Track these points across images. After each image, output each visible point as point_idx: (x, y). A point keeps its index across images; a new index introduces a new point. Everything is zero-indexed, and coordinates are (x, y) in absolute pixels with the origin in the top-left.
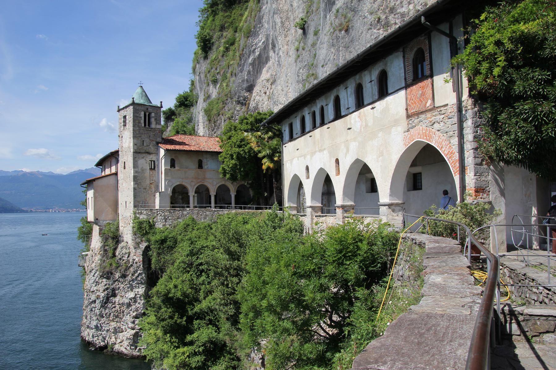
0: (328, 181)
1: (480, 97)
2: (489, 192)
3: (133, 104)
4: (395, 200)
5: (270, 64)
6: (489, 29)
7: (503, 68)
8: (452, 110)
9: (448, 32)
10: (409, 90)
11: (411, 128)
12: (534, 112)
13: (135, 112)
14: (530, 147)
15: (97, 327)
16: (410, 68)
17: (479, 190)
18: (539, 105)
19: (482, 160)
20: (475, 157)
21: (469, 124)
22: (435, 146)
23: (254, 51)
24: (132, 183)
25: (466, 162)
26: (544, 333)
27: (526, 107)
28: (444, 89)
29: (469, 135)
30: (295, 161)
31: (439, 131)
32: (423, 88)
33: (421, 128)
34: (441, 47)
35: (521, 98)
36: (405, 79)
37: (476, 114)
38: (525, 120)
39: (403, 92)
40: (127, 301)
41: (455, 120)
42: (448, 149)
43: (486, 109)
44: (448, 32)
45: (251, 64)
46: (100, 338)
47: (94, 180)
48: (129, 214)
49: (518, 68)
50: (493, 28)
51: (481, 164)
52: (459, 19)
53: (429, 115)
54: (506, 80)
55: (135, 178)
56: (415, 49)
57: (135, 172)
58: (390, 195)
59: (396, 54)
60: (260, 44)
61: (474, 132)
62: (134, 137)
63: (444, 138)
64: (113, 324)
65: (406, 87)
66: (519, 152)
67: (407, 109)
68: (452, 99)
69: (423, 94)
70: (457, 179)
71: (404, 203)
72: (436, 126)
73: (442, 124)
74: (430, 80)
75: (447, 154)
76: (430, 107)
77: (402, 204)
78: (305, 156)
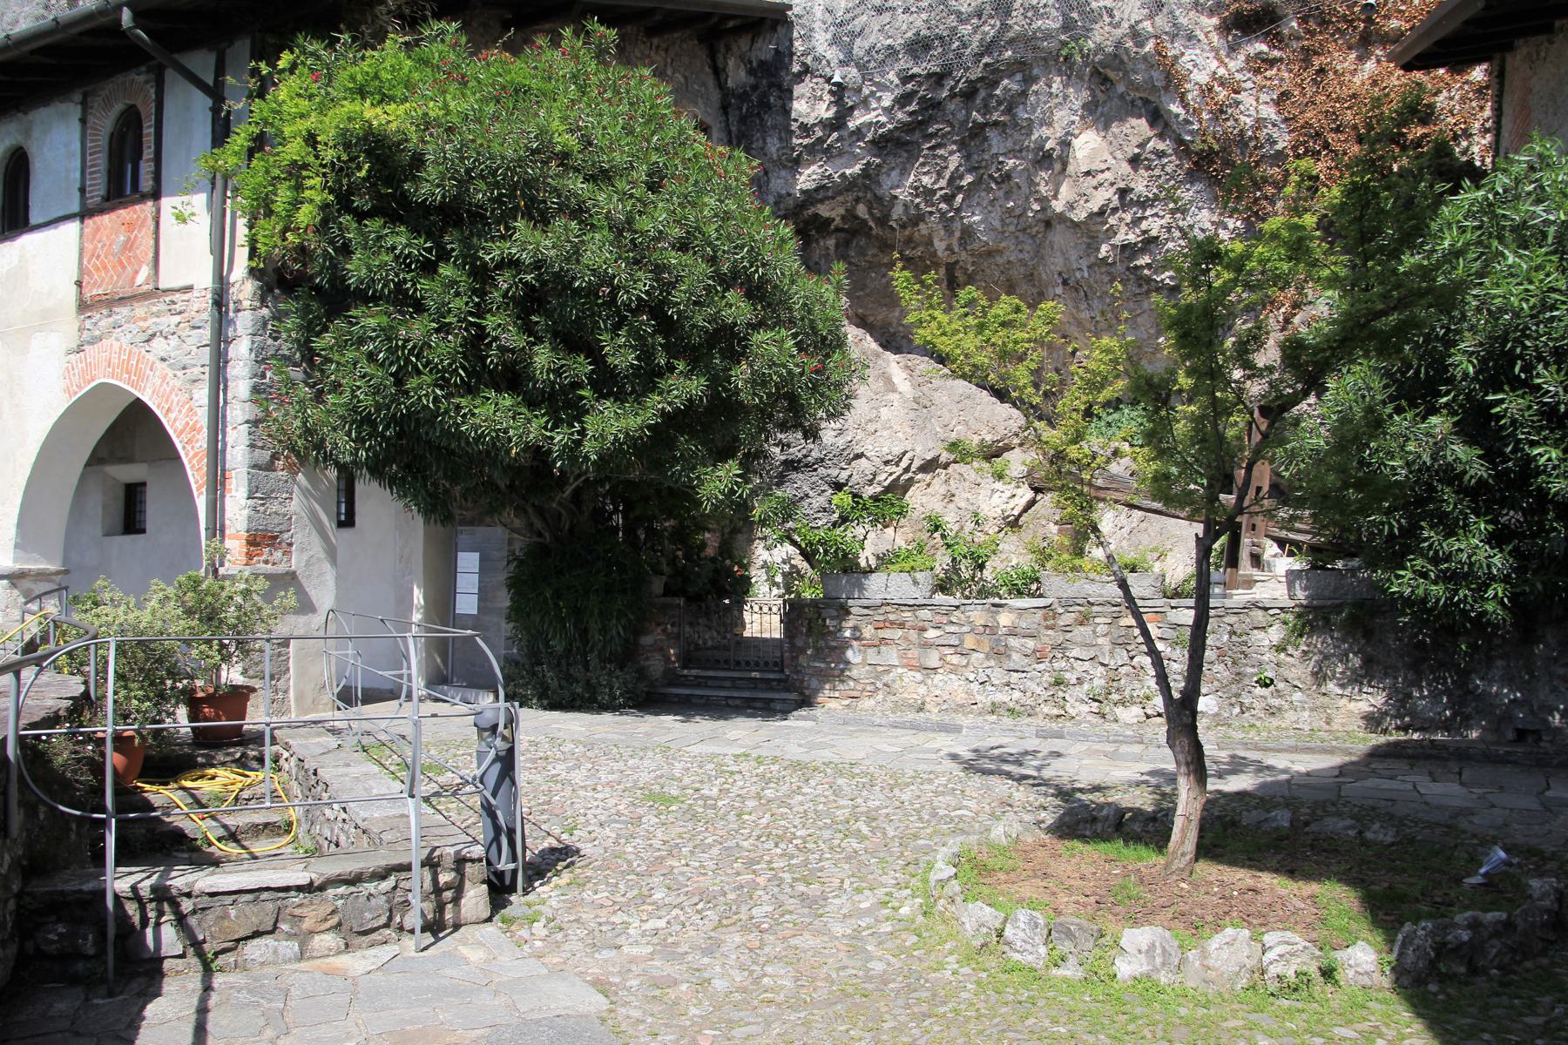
1: (276, 280)
2: (291, 545)
4: (36, 561)
6: (299, 95)
7: (325, 207)
8: (201, 304)
9: (210, 82)
10: (89, 222)
11: (89, 343)
12: (389, 339)
14: (387, 427)
16: (101, 162)
17: (259, 540)
18: (402, 322)
19: (275, 457)
20: (252, 446)
21: (241, 350)
22: (150, 404)
25: (228, 457)
26: (247, 938)
27: (372, 322)
28: (187, 239)
29: (240, 382)
31: (163, 360)
32: (130, 226)
33: (116, 345)
34: (186, 113)
35: (365, 297)
36: (82, 190)
37: (265, 324)
38: (371, 357)
39: (73, 227)
41: (206, 334)
42: (182, 416)
43: (287, 314)
44: (210, 82)
49: (360, 216)
50: (311, 97)
51: (270, 467)
52: (243, 46)
53: (140, 309)
54: (332, 242)
56: (118, 107)
58: (16, 546)
59: (62, 107)
61: (255, 376)
63: (178, 383)
65: (84, 214)
66: (360, 440)
67: (79, 284)
68: (203, 277)
69: (129, 246)
70: (201, 502)
71: (66, 572)
72: (158, 345)
73: (174, 341)
74: (150, 203)
75: (182, 432)
76: (145, 288)
77: (58, 573)
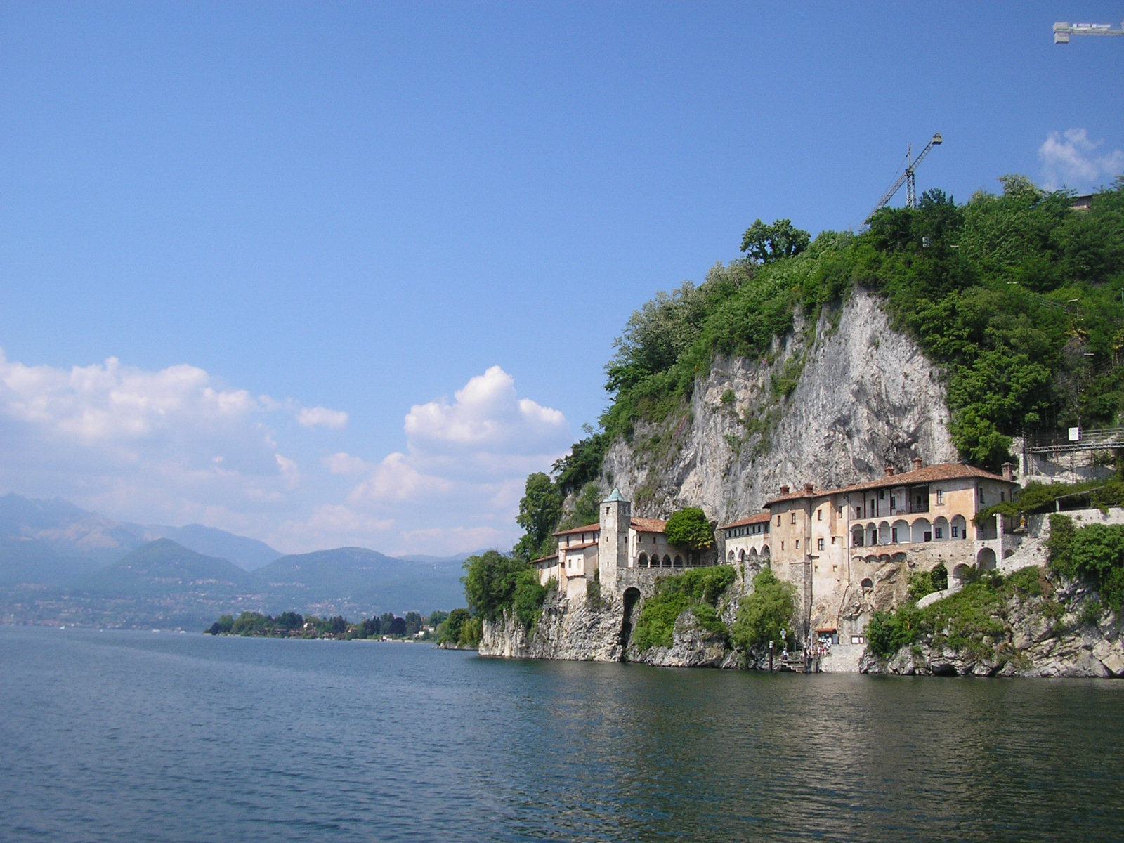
0: (744, 552)
3: (618, 501)
5: (697, 469)
13: (619, 506)
15: (581, 646)
23: (684, 460)
24: (616, 551)
30: (732, 545)
40: (609, 626)
45: (681, 468)
46: (582, 654)
47: (585, 548)
48: (611, 570)
55: (618, 548)
57: (618, 544)
60: (690, 456)
62: (618, 522)
64: (595, 643)
78: (735, 544)
